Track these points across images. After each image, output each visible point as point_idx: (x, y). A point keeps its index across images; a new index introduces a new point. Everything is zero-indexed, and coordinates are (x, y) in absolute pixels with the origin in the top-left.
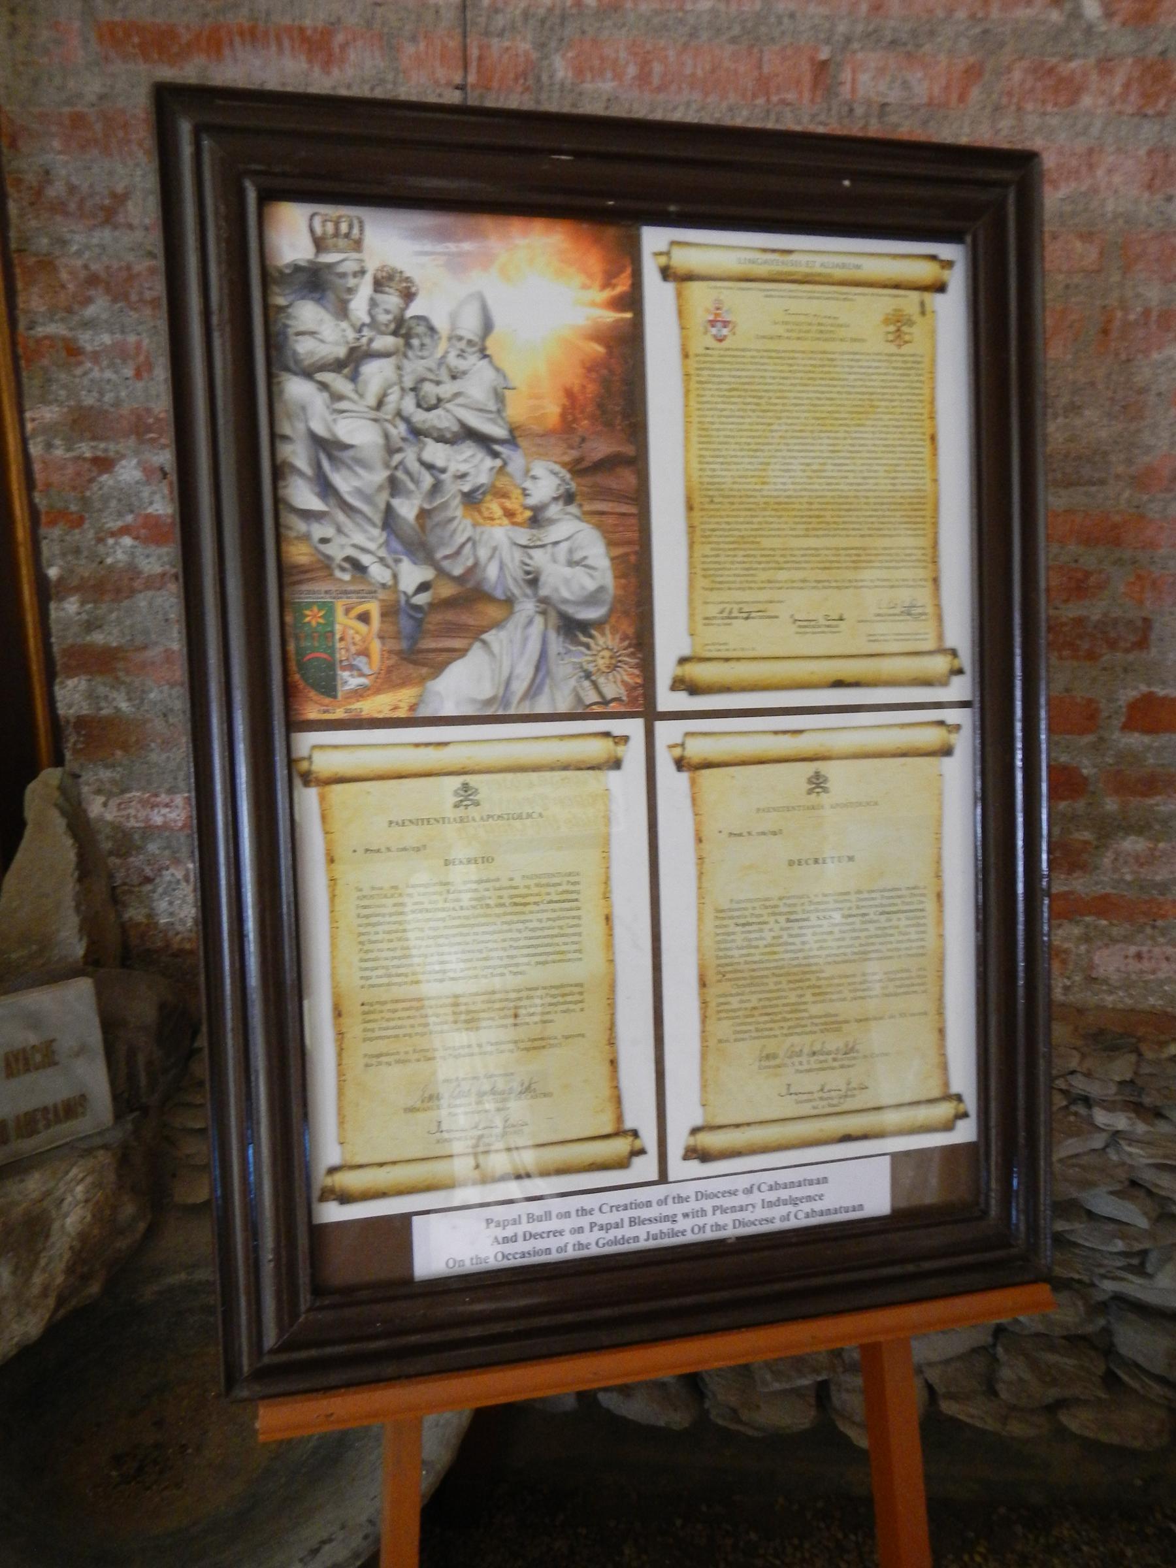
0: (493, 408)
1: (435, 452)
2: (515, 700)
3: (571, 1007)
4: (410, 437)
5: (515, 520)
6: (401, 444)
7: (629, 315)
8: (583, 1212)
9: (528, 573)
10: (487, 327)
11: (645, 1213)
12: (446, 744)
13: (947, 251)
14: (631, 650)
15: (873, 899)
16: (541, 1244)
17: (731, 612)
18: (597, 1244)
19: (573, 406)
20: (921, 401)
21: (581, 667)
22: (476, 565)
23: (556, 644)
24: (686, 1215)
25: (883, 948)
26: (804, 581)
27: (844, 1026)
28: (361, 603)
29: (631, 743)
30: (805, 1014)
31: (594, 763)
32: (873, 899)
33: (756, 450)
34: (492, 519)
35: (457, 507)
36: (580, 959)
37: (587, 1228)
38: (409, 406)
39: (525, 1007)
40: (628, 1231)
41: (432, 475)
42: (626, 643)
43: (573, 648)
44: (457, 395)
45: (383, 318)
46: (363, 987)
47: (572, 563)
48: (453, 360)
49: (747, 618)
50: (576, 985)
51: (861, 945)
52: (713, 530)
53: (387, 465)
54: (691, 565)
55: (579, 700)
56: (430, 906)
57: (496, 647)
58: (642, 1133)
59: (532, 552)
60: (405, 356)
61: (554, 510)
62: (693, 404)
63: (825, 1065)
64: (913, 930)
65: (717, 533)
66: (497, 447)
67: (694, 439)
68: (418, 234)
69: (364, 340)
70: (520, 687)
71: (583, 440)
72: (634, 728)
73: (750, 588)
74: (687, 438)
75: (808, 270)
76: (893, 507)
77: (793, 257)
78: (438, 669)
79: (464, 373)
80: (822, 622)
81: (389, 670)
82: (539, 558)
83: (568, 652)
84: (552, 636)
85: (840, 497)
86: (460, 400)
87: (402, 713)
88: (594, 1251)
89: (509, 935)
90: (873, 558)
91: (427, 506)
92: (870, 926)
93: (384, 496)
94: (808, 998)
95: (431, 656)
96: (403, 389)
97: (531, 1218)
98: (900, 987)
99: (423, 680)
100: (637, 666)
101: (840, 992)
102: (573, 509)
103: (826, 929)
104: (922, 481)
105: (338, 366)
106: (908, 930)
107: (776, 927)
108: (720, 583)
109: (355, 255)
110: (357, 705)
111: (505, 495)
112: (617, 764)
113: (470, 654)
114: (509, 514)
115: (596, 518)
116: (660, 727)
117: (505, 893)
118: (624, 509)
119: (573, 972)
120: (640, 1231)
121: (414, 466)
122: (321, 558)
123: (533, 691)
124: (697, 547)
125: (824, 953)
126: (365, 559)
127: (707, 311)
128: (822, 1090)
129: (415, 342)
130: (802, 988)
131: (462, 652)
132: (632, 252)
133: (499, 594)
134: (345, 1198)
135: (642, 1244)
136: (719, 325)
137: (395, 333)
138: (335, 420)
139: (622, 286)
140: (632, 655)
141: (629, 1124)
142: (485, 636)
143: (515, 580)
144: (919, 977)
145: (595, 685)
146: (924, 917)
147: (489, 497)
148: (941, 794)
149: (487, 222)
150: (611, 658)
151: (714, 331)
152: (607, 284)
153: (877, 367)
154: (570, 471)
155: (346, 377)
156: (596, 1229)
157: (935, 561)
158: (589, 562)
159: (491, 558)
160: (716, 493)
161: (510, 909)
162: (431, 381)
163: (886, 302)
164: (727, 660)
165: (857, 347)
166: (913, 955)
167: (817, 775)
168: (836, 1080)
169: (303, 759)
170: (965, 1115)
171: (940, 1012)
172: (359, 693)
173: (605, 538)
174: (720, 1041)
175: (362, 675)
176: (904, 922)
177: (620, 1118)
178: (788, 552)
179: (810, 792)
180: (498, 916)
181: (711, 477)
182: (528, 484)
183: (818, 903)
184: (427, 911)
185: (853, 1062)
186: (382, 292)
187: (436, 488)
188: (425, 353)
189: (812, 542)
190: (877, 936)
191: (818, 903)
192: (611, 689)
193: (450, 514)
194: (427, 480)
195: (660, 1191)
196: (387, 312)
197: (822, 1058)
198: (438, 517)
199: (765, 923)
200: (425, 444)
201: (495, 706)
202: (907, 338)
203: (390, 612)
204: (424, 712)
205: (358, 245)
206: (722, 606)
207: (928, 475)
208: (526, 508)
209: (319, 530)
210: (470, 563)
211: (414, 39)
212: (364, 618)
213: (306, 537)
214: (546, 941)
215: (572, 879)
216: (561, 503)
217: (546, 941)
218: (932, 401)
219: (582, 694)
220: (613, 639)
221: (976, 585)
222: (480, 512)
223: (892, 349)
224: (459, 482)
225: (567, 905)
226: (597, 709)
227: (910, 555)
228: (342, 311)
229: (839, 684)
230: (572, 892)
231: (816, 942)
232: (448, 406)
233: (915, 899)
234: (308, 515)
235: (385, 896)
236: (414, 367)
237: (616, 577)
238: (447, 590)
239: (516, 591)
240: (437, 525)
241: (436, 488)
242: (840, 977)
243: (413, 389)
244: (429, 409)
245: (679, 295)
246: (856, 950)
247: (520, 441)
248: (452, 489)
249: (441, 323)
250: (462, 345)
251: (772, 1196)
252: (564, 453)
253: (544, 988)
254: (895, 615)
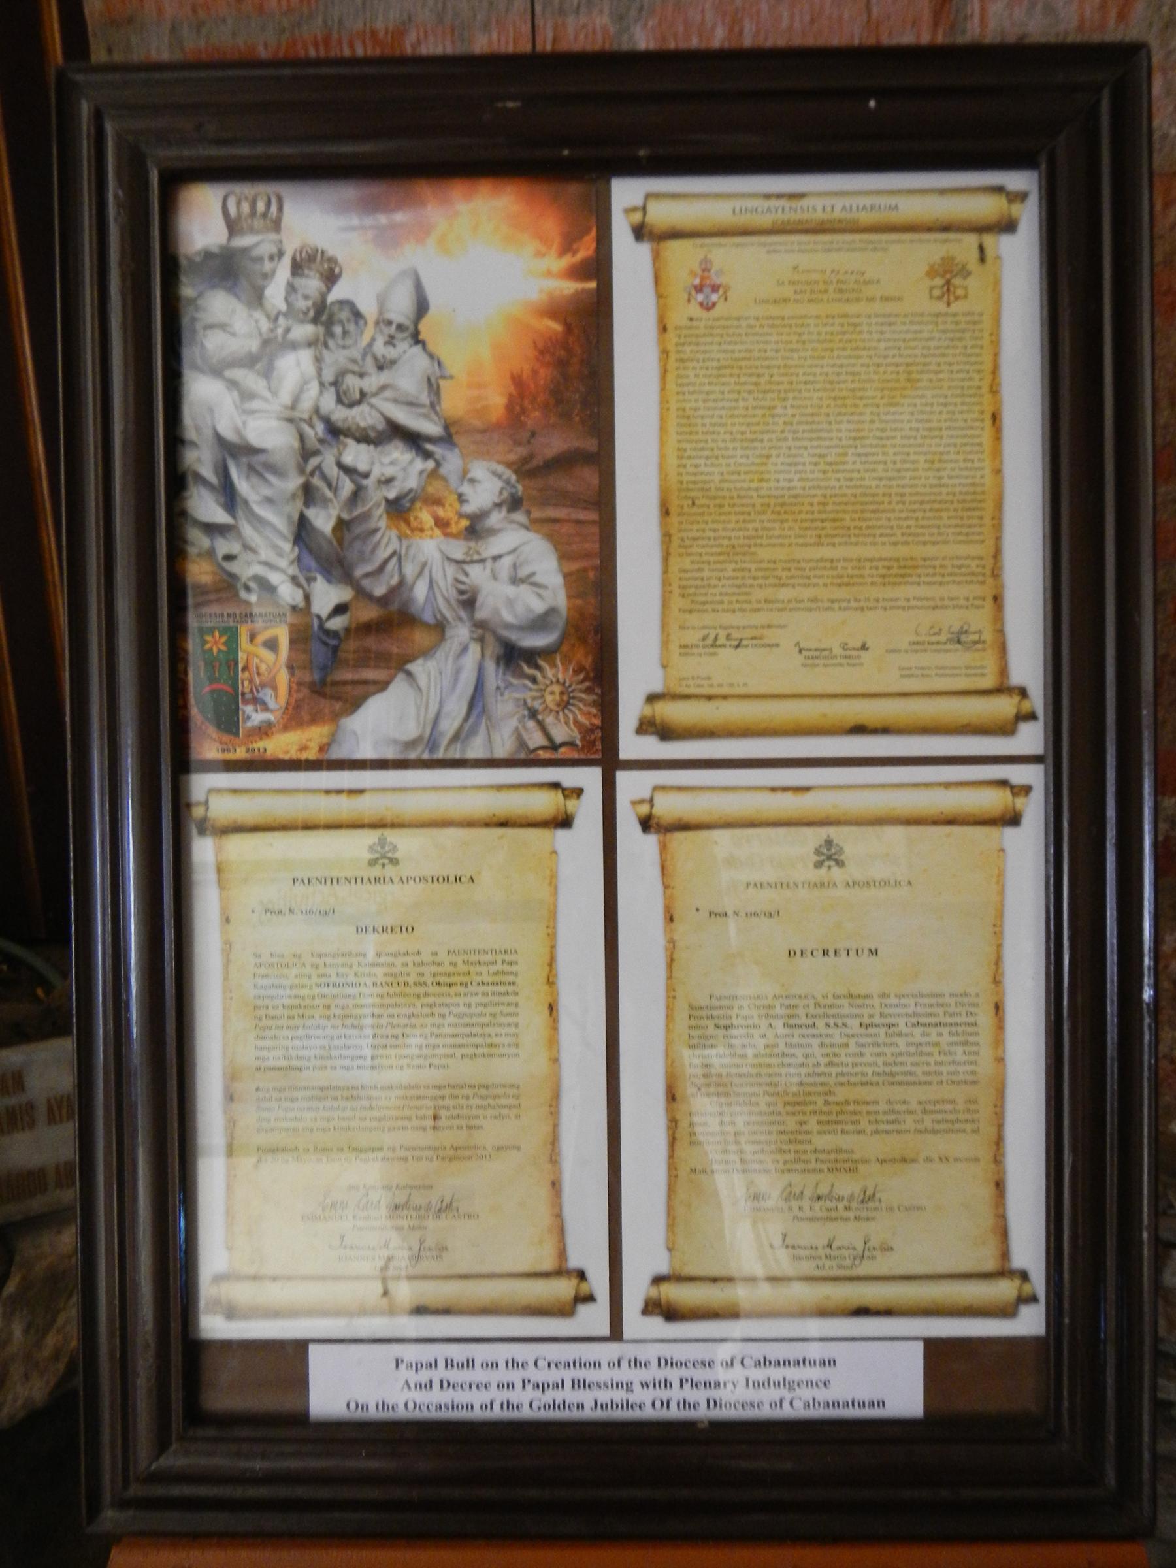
0: (427, 402)
1: (356, 454)
2: (444, 742)
3: (505, 1112)
4: (329, 438)
5: (449, 530)
6: (318, 446)
7: (593, 285)
8: (513, 1364)
9: (461, 592)
10: (422, 307)
11: (591, 1375)
12: (361, 791)
13: (1021, 180)
14: (587, 684)
15: (904, 1006)
16: (462, 1397)
17: (716, 639)
18: (531, 1405)
19: (522, 396)
20: (979, 372)
21: (525, 702)
22: (402, 582)
23: (494, 676)
24: (645, 1385)
25: (919, 1070)
26: (814, 600)
27: (861, 1167)
28: (266, 628)
29: (584, 797)
30: (808, 1147)
31: (539, 818)
32: (904, 1006)
33: (752, 441)
34: (422, 530)
35: (380, 517)
36: (517, 1055)
37: (519, 1385)
38: (328, 402)
39: (448, 1108)
40: (570, 1395)
41: (353, 481)
42: (581, 676)
43: (515, 681)
44: (383, 388)
45: (302, 304)
46: (258, 1069)
47: (515, 581)
48: (380, 348)
49: (737, 647)
50: (512, 1086)
51: (886, 1064)
52: (695, 539)
53: (302, 471)
54: (666, 582)
55: (522, 744)
56: (338, 981)
57: (422, 681)
58: (590, 1274)
59: (466, 567)
60: (326, 345)
61: (496, 519)
62: (671, 386)
63: (833, 1214)
64: (960, 1049)
65: (700, 542)
66: (429, 447)
67: (672, 428)
68: (343, 208)
69: (280, 331)
70: (449, 726)
71: (533, 434)
72: (590, 778)
73: (742, 610)
74: (663, 429)
75: (825, 216)
76: (936, 506)
77: (805, 202)
78: (355, 704)
79: (393, 362)
80: (837, 651)
81: (298, 706)
82: (477, 575)
83: (509, 685)
84: (490, 666)
85: (865, 495)
86: (388, 394)
87: (311, 755)
88: (526, 1413)
89: (429, 1021)
90: (909, 571)
91: (345, 516)
92: (901, 1042)
93: (299, 504)
94: (812, 1124)
95: (349, 688)
96: (322, 384)
97: (449, 1363)
98: (938, 1122)
99: (336, 717)
100: (594, 704)
101: (857, 1122)
102: (520, 516)
103: (837, 1039)
104: (979, 474)
105: (250, 361)
106: (953, 1049)
107: (770, 1033)
108: (704, 603)
109: (273, 236)
110: (260, 745)
111: (438, 502)
112: (565, 822)
113: (392, 687)
114: (441, 524)
115: (545, 526)
116: (622, 777)
117: (427, 970)
118: (582, 515)
119: (504, 1070)
120: (586, 1397)
121: (333, 471)
122: (225, 577)
124: (672, 560)
125: (834, 1070)
126: (275, 578)
127: (693, 274)
128: (830, 1246)
129: (338, 330)
130: (804, 1113)
131: (383, 686)
133: (428, 617)
134: (231, 1313)
135: (588, 1414)
136: (707, 290)
137: (315, 321)
138: (244, 423)
139: (586, 250)
140: (589, 691)
141: (574, 1262)
142: (409, 667)
143: (447, 601)
144: (969, 1111)
145: (542, 726)
146: (977, 1034)
147: (418, 505)
148: (1001, 875)
149: (424, 188)
150: (562, 693)
151: (700, 297)
152: (567, 248)
153: (916, 332)
154: (516, 472)
155: (259, 374)
156: (529, 1387)
157: (996, 573)
158: (538, 579)
159: (420, 573)
160: (700, 494)
161: (431, 990)
162: (354, 373)
163: (933, 249)
164: (710, 698)
165: (889, 308)
166: (959, 1083)
167: (829, 843)
168: (849, 1234)
169: (198, 804)
170: (1033, 1299)
171: (998, 1158)
172: (264, 731)
173: (556, 549)
174: (693, 1171)
175: (266, 708)
176: (946, 1038)
177: (562, 1253)
178: (793, 565)
179: (819, 865)
180: (418, 996)
181: (695, 474)
182: (466, 489)
183: (830, 1006)
184: (334, 985)
185: (871, 1214)
186: (302, 275)
187: (356, 496)
188: (349, 342)
189: (826, 552)
190: (908, 1054)
191: (830, 1006)
192: (560, 733)
193: (372, 524)
194: (347, 487)
195: (611, 1350)
196: (306, 297)
197: (829, 1204)
198: (358, 530)
199: (755, 1026)
200: (345, 445)
201: (420, 749)
202: (960, 292)
203: (299, 638)
204: (336, 753)
205: (277, 225)
206: (705, 632)
207: (987, 464)
208: (461, 516)
209: (223, 546)
210: (395, 581)
211: (486, 26)
212: (272, 645)
213: (211, 553)
214: (475, 1030)
215: (508, 958)
216: (504, 509)
217: (475, 1030)
218: (995, 370)
219: (525, 736)
220: (566, 670)
221: (1049, 607)
222: (408, 523)
223: (941, 307)
224: (384, 488)
225: (501, 989)
226: (543, 755)
227: (960, 567)
228: (257, 299)
229: (859, 729)
230: (508, 973)
231: (823, 1056)
232: (374, 401)
233: (963, 1010)
234: (212, 529)
235: (287, 965)
236: (336, 358)
237: (569, 597)
238: (368, 613)
239: (448, 614)
240: (358, 537)
242: (856, 1102)
243: (335, 384)
244: (351, 405)
245: (656, 256)
246: (880, 1070)
247: (456, 439)
248: (376, 497)
249: (368, 307)
250: (392, 329)
251: (759, 1374)
252: (511, 451)
253: (472, 1087)
254: (938, 643)
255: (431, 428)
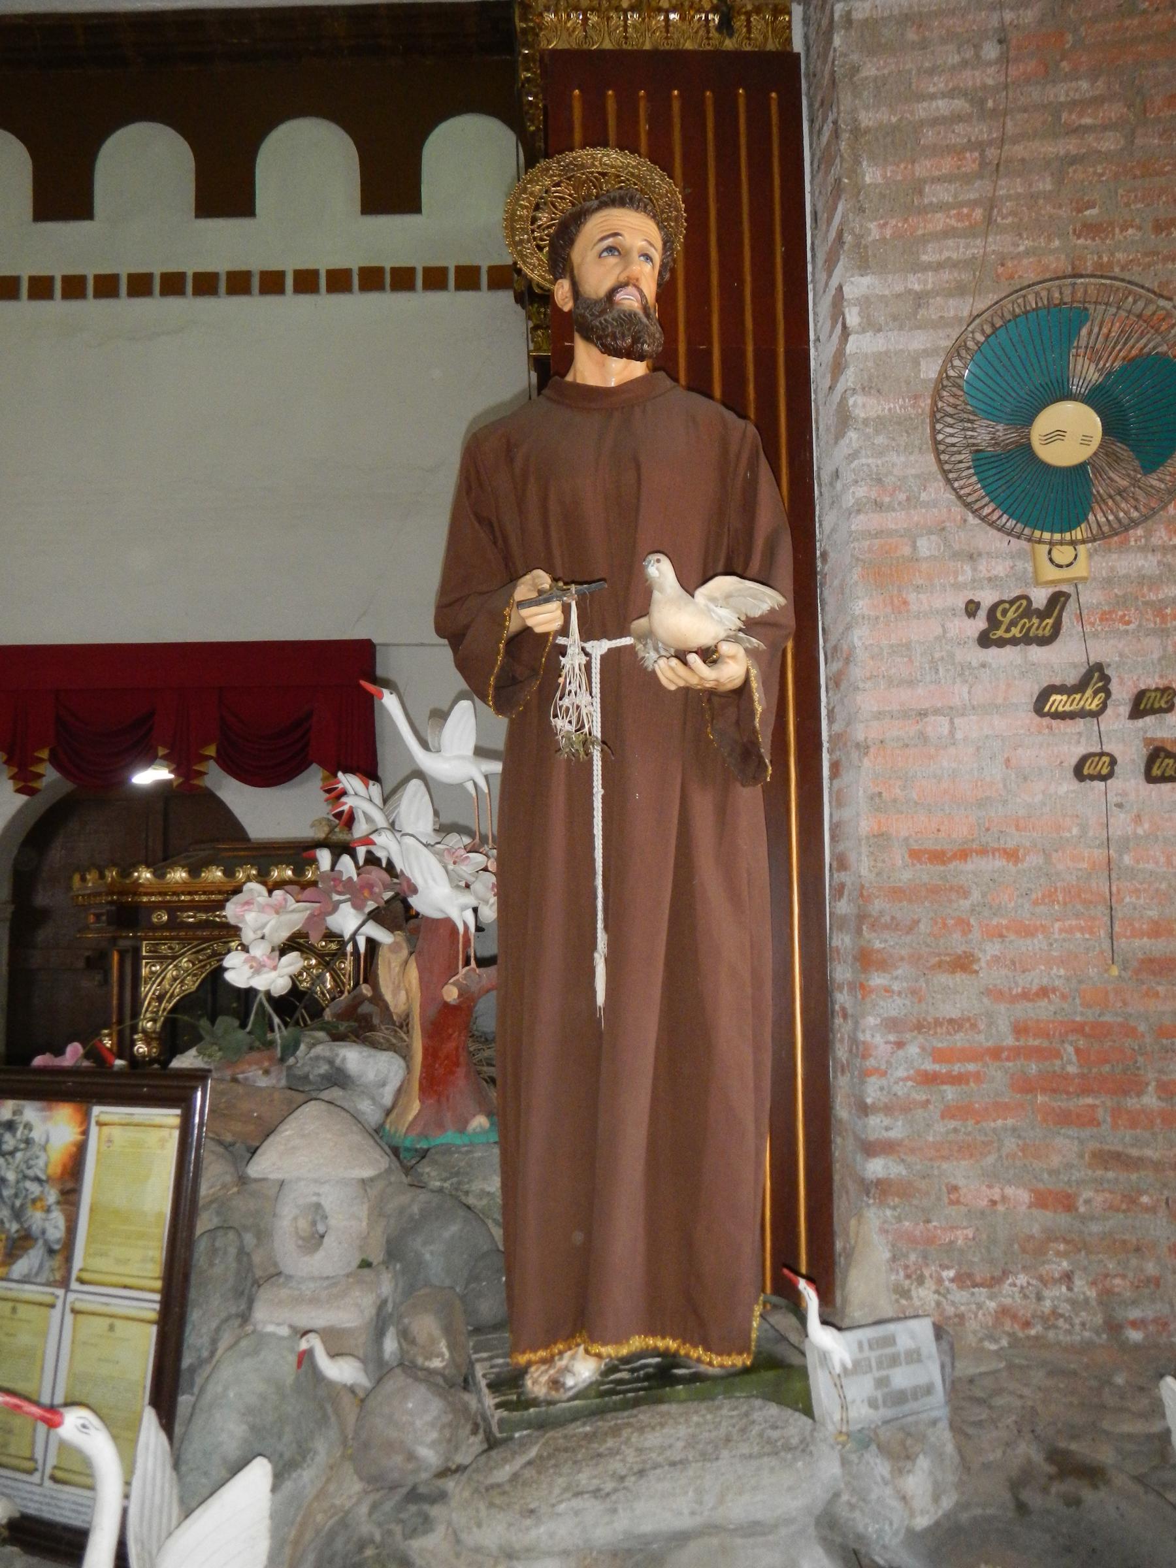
10: (47, 1141)
23: (46, 1257)
61: (53, 1207)
70: (34, 1271)
72: (60, 1292)
82: (47, 1225)
123: (37, 1274)
132: (86, 1117)
228: (14, 1136)
238: (23, 1233)
241: (26, 1197)
249: (37, 1140)
255: (43, 1177)
